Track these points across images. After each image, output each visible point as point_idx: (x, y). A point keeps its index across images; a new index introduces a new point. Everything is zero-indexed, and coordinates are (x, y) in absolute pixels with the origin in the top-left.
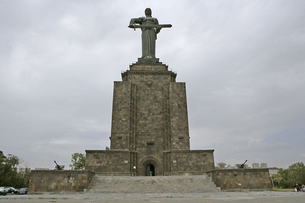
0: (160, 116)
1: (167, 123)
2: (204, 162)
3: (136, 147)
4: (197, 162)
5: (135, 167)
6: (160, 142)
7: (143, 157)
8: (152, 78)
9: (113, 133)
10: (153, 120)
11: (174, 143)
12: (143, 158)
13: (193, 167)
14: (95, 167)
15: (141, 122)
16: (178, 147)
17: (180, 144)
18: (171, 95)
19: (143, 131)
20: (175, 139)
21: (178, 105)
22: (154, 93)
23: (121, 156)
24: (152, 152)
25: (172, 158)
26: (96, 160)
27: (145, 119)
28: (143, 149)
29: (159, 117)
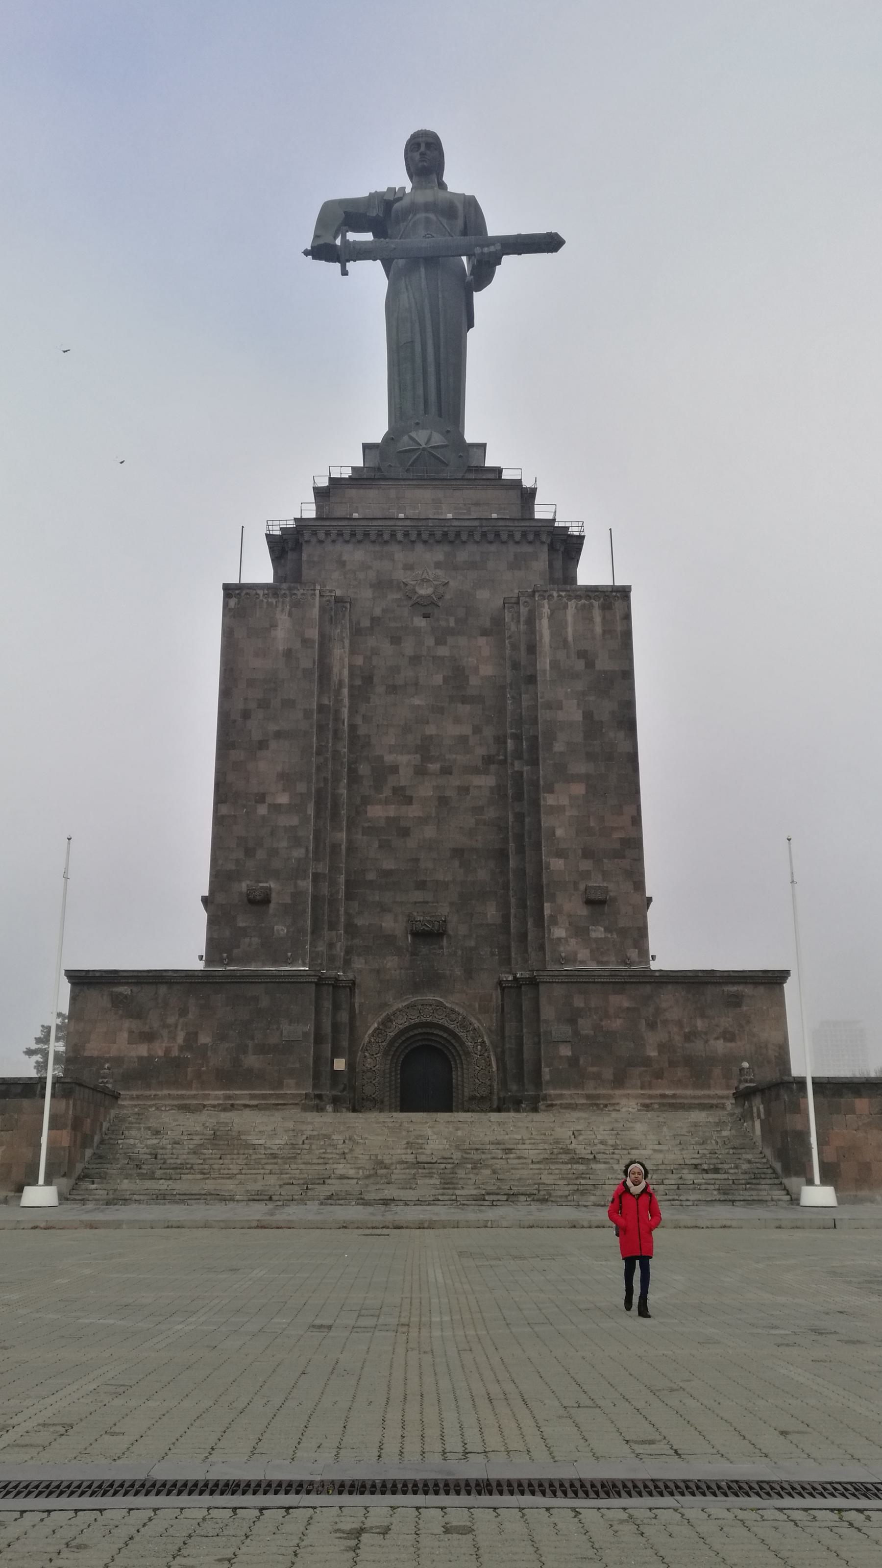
0: (486, 781)
1: (520, 817)
2: (728, 1036)
3: (348, 951)
5: (340, 1064)
7: (385, 1005)
8: (438, 565)
9: (220, 877)
10: (443, 801)
11: (559, 932)
12: (386, 1006)
13: (667, 1065)
14: (118, 1061)
15: (376, 812)
17: (593, 935)
18: (544, 663)
19: (388, 864)
20: (568, 907)
21: (588, 716)
23: (265, 1003)
24: (432, 980)
25: (548, 1012)
26: (127, 1024)
27: (403, 797)
28: (389, 965)
29: (480, 787)
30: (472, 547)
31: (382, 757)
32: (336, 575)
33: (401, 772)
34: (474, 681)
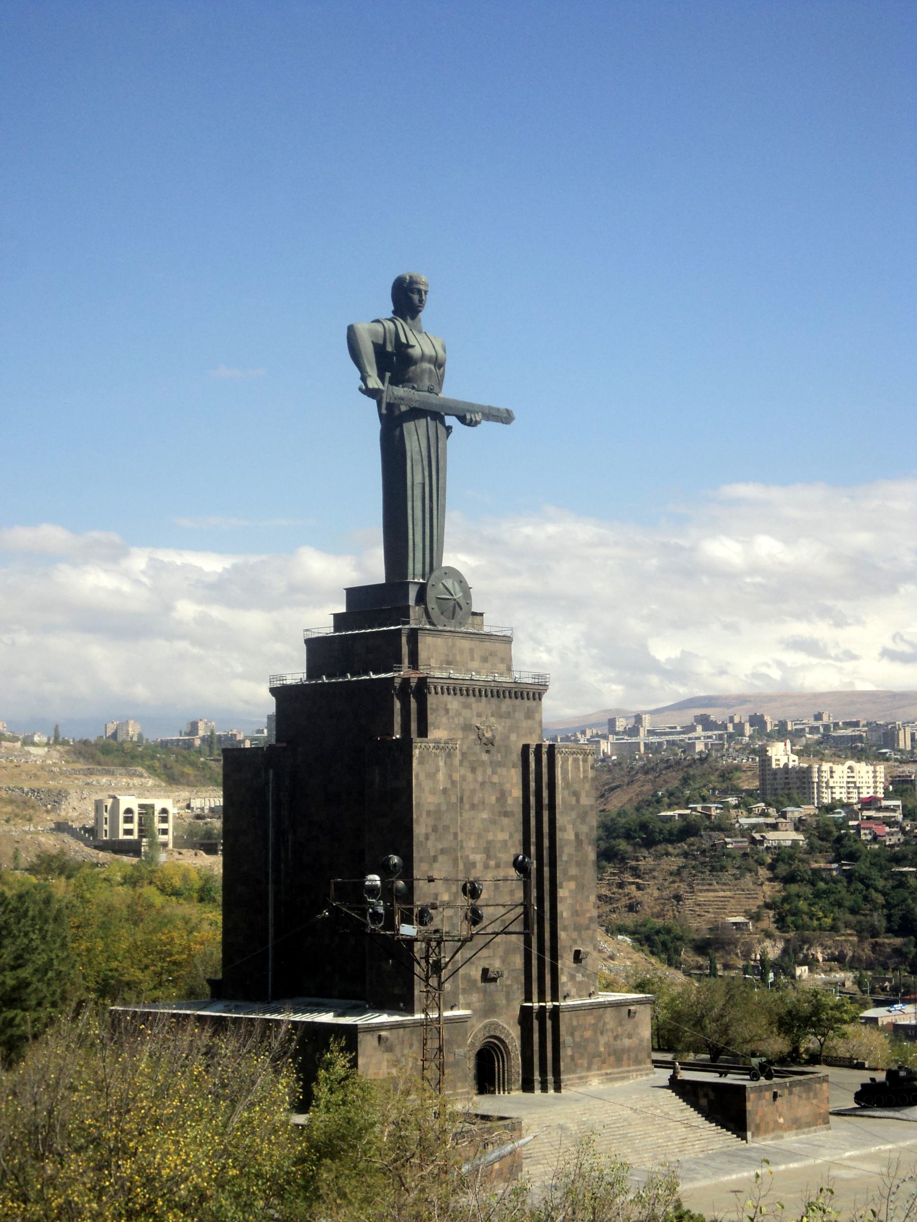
2: (630, 1036)
4: (616, 1038)
6: (513, 970)
16: (573, 992)
17: (578, 979)
21: (577, 835)
22: (500, 776)
26: (387, 1056)
30: (507, 700)
31: (468, 856)
32: (444, 720)
33: (477, 864)
34: (510, 801)
